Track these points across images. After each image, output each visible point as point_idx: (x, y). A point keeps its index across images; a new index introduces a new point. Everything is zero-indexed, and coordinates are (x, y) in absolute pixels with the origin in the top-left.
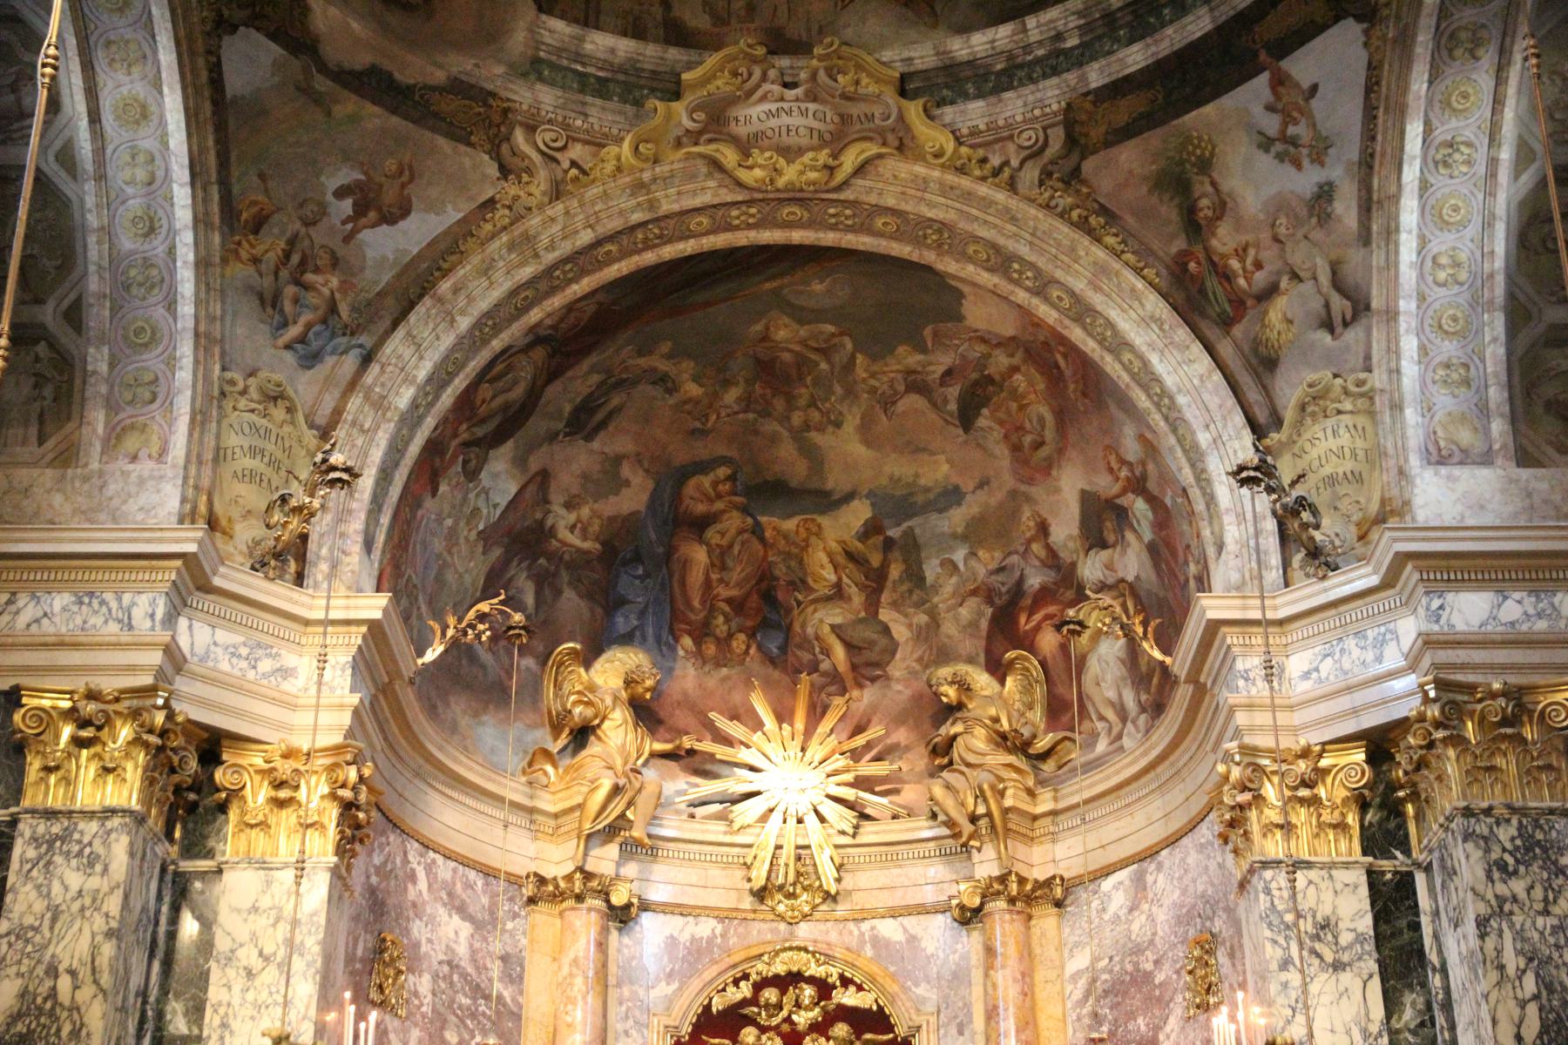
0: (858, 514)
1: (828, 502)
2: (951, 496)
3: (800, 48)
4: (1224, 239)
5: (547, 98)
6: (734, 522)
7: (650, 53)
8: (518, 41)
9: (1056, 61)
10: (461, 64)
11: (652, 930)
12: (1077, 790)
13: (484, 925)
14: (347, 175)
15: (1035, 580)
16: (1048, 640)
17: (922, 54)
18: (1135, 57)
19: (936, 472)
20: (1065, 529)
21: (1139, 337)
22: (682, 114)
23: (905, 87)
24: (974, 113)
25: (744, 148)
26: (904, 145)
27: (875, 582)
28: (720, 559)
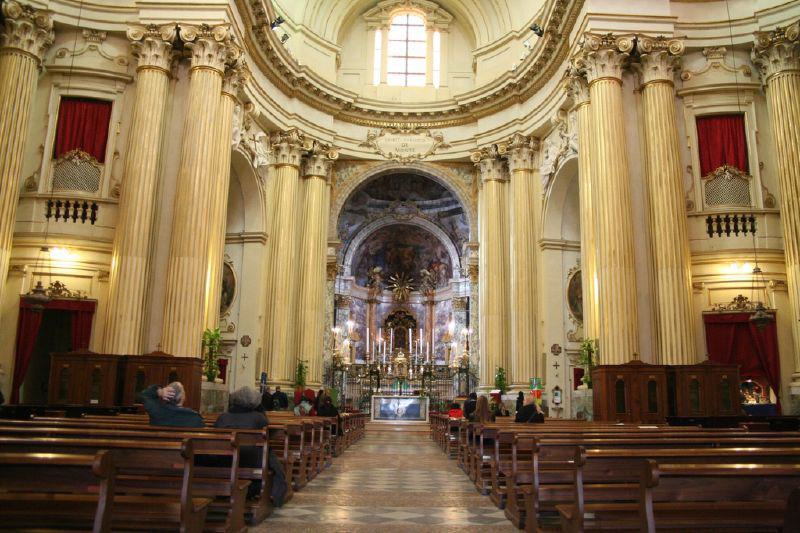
0: (411, 248)
1: (407, 246)
2: (423, 248)
3: (404, 200)
4: (457, 231)
5: (372, 209)
6: (393, 249)
7: (384, 201)
8: (368, 203)
9: (437, 206)
10: (361, 207)
11: (383, 305)
12: (437, 291)
13: (361, 306)
14: (347, 222)
15: (435, 260)
16: (436, 268)
17: (420, 203)
18: (446, 209)
19: (421, 245)
20: (439, 254)
21: (446, 243)
22: (389, 210)
23: (418, 207)
24: (427, 211)
25: (397, 214)
26: (417, 215)
27: (413, 258)
28: (392, 254)
